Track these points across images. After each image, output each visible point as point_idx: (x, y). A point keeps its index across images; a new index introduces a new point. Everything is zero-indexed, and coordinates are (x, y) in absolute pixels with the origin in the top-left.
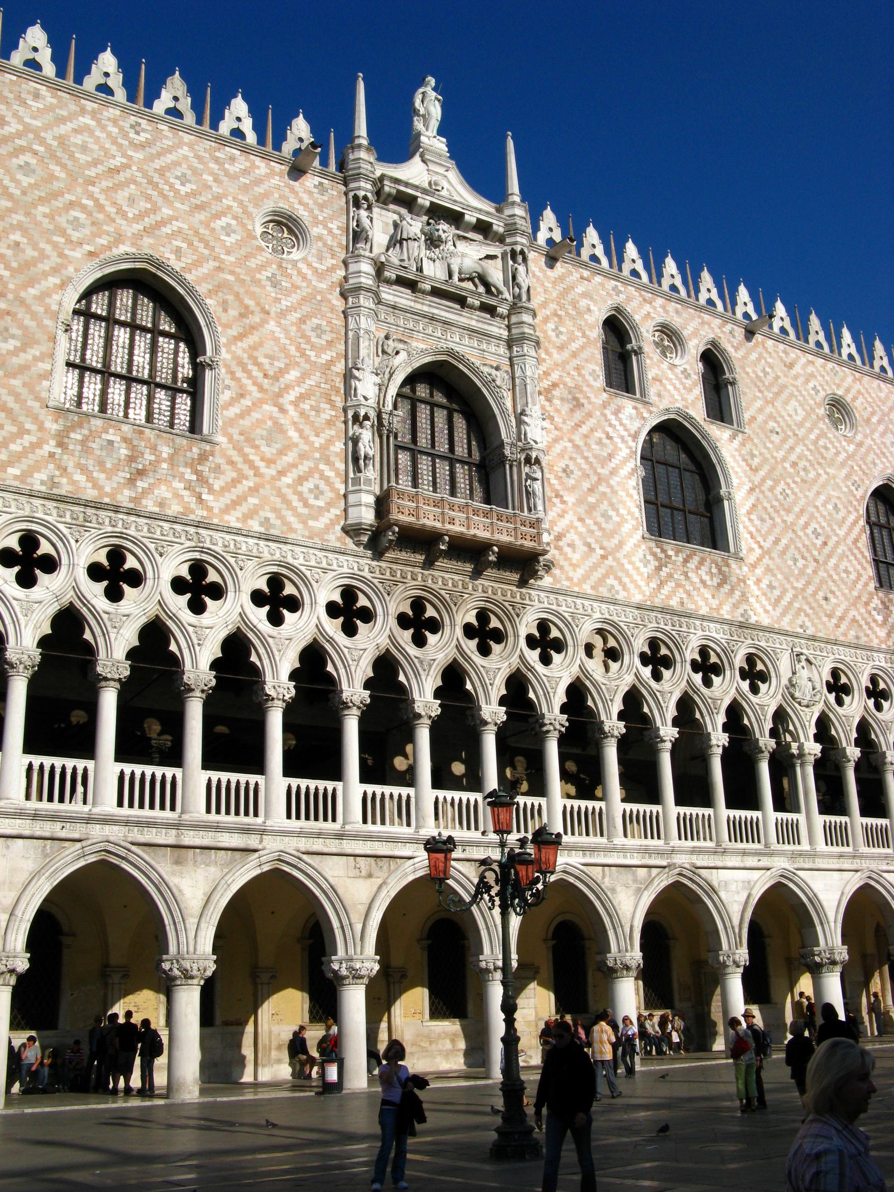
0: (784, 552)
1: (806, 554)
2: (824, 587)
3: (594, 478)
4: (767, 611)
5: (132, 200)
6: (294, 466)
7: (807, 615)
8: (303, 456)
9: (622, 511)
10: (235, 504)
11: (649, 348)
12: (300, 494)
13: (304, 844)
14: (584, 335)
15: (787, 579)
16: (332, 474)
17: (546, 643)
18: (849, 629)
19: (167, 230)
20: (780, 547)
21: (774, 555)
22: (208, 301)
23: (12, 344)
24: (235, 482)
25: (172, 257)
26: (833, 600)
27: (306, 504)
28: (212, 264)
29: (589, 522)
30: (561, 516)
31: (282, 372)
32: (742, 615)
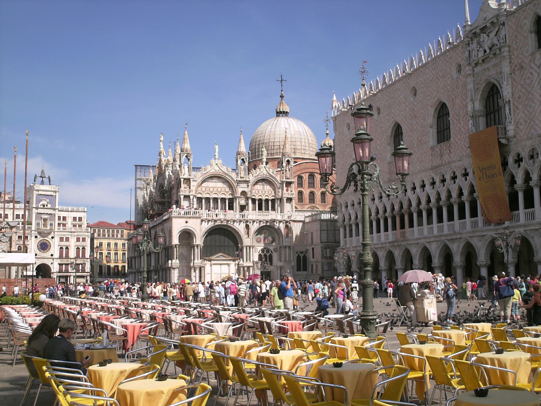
3: (527, 94)
8: (464, 134)
9: (536, 101)
17: (519, 160)
30: (518, 115)
31: (460, 112)
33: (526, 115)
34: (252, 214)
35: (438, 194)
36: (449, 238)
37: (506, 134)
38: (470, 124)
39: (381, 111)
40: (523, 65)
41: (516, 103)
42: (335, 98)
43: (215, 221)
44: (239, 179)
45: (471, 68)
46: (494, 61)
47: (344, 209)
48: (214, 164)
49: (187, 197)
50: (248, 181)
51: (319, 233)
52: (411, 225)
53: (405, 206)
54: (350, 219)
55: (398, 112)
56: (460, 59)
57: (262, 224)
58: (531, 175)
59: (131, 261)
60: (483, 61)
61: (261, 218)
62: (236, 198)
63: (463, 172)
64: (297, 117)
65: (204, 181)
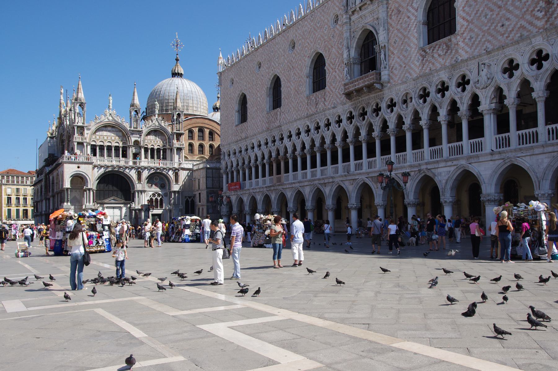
0: (480, 16)
1: (493, 7)
2: (503, 19)
3: (403, 38)
4: (467, 52)
7: (489, 41)
13: (341, 179)
15: (480, 29)
17: (392, 105)
18: (515, 35)
20: (478, 15)
21: (475, 21)
26: (507, 23)
29: (401, 56)
30: (393, 60)
32: (455, 60)
33: (401, 60)
34: (144, 162)
35: (313, 141)
36: (322, 182)
37: (380, 79)
38: (345, 72)
39: (262, 65)
40: (401, 9)
41: (392, 49)
42: (221, 56)
43: (108, 167)
44: (132, 129)
45: (348, 16)
46: (371, 8)
47: (226, 157)
48: (108, 114)
49: (80, 144)
50: (140, 131)
51: (205, 179)
52: (287, 171)
53: (282, 153)
54: (232, 166)
55: (277, 65)
56: (337, 9)
57: (152, 171)
58: (404, 120)
59: (37, 204)
60: (360, 8)
61: (152, 165)
62: (129, 146)
63: (337, 119)
64: (191, 78)
65: (98, 130)
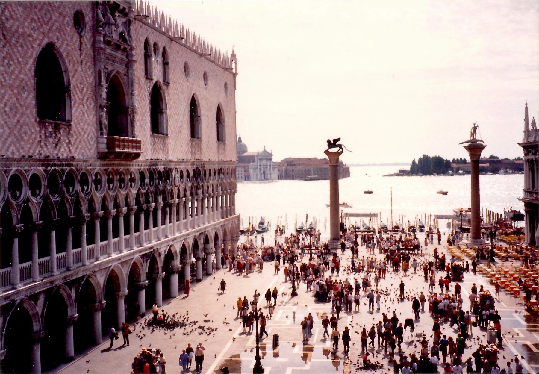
5: (45, 14)
6: (87, 129)
8: (88, 125)
10: (77, 148)
11: (153, 54)
12: (88, 140)
14: (141, 54)
16: (94, 130)
19: (54, 28)
22: (66, 61)
23: (26, 93)
24: (76, 139)
25: (56, 41)
27: (90, 144)
28: (66, 42)
31: (83, 89)
